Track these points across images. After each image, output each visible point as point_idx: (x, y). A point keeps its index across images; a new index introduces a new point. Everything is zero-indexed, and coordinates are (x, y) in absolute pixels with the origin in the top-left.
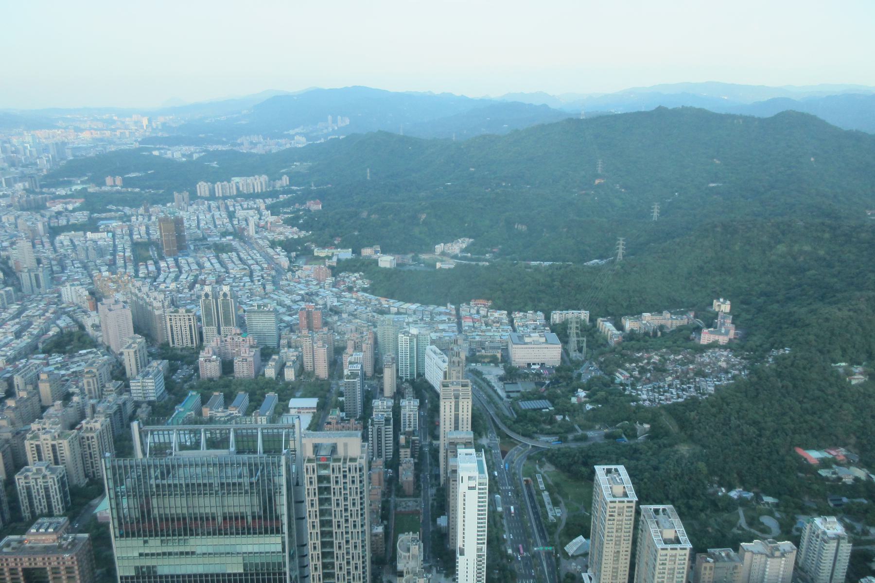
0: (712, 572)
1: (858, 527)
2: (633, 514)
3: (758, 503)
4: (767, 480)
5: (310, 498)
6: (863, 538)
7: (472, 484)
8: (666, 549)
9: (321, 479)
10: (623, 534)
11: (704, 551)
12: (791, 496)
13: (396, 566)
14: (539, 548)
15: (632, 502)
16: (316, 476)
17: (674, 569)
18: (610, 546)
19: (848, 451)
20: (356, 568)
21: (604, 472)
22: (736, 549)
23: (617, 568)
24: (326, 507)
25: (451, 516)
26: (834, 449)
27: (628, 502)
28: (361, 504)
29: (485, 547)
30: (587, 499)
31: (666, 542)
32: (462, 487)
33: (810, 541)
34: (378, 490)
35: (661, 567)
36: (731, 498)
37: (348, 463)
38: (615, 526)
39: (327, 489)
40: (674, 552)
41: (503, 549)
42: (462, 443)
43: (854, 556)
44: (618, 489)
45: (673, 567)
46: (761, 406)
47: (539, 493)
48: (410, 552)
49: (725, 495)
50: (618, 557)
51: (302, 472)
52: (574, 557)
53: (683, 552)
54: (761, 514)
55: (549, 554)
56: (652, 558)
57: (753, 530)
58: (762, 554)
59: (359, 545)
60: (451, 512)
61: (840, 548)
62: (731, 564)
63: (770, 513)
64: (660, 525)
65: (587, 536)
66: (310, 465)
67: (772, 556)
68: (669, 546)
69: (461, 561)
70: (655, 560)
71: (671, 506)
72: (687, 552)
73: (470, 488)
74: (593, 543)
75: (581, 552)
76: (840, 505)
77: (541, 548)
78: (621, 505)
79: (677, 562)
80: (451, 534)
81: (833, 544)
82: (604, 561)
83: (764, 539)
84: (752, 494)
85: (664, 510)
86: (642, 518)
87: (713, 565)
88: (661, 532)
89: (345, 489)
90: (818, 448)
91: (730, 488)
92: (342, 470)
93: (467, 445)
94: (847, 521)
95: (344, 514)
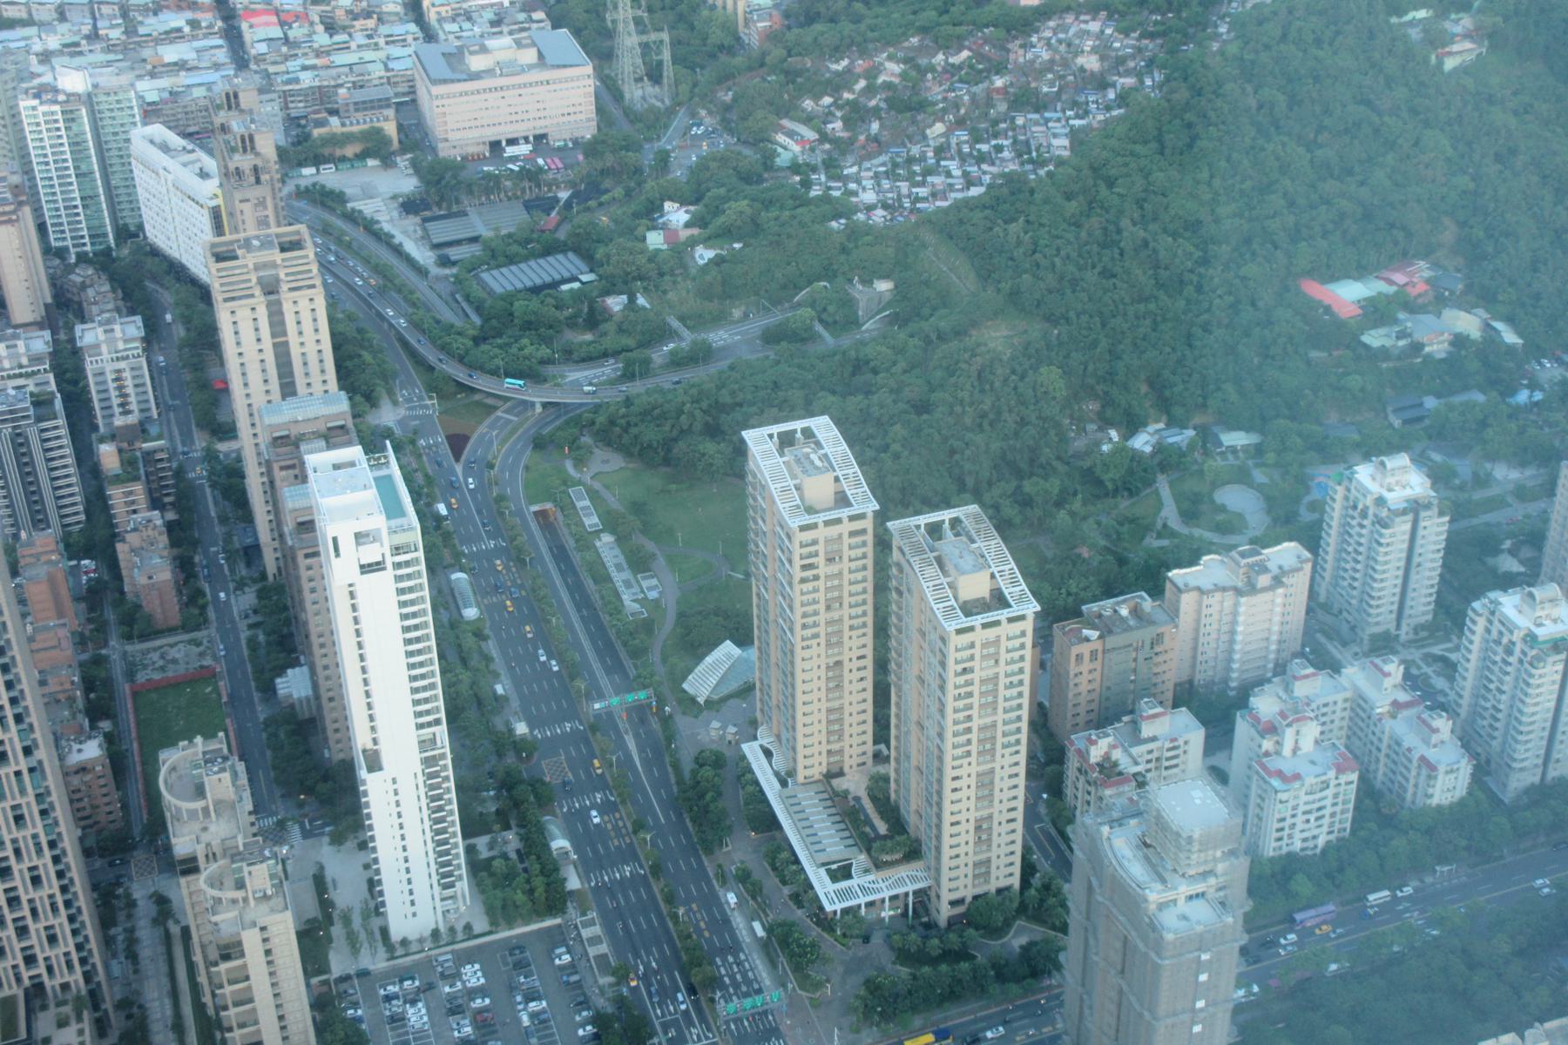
0: (1097, 665)
1: (1464, 468)
2: (869, 550)
3: (1206, 453)
4: (1229, 388)
6: (1477, 496)
7: (371, 554)
8: (971, 629)
10: (846, 611)
12: (1293, 418)
13: (168, 848)
14: (611, 702)
15: (862, 516)
17: (996, 676)
18: (814, 651)
19: (1436, 265)
20: (36, 881)
21: (772, 446)
22: (1156, 589)
23: (841, 708)
25: (320, 663)
26: (1397, 270)
27: (852, 518)
29: (442, 732)
31: (969, 609)
32: (341, 571)
33: (1345, 532)
35: (961, 680)
36: (1136, 456)
38: (821, 596)
40: (991, 633)
42: (318, 435)
43: (1454, 548)
44: (820, 488)
45: (991, 673)
46: (1205, 175)
47: (585, 541)
48: (206, 795)
49: (1120, 450)
53: (1017, 627)
54: (1215, 485)
55: (639, 711)
56: (935, 661)
57: (1197, 532)
58: (1224, 589)
59: (31, 808)
60: (317, 652)
61: (1421, 532)
62: (1147, 634)
63: (1241, 477)
64: (949, 567)
65: (743, 640)
67: (1251, 589)
68: (977, 621)
69: (374, 787)
70: (943, 664)
72: (1028, 626)
73: (367, 569)
74: (764, 654)
75: (734, 685)
76: (1420, 419)
77: (615, 701)
78: (833, 531)
80: (329, 717)
81: (1403, 527)
82: (800, 699)
84: (1190, 433)
85: (955, 522)
86: (896, 554)
87: (1098, 645)
88: (952, 586)
90: (1360, 271)
91: (1132, 425)
93: (332, 436)
94: (1437, 457)
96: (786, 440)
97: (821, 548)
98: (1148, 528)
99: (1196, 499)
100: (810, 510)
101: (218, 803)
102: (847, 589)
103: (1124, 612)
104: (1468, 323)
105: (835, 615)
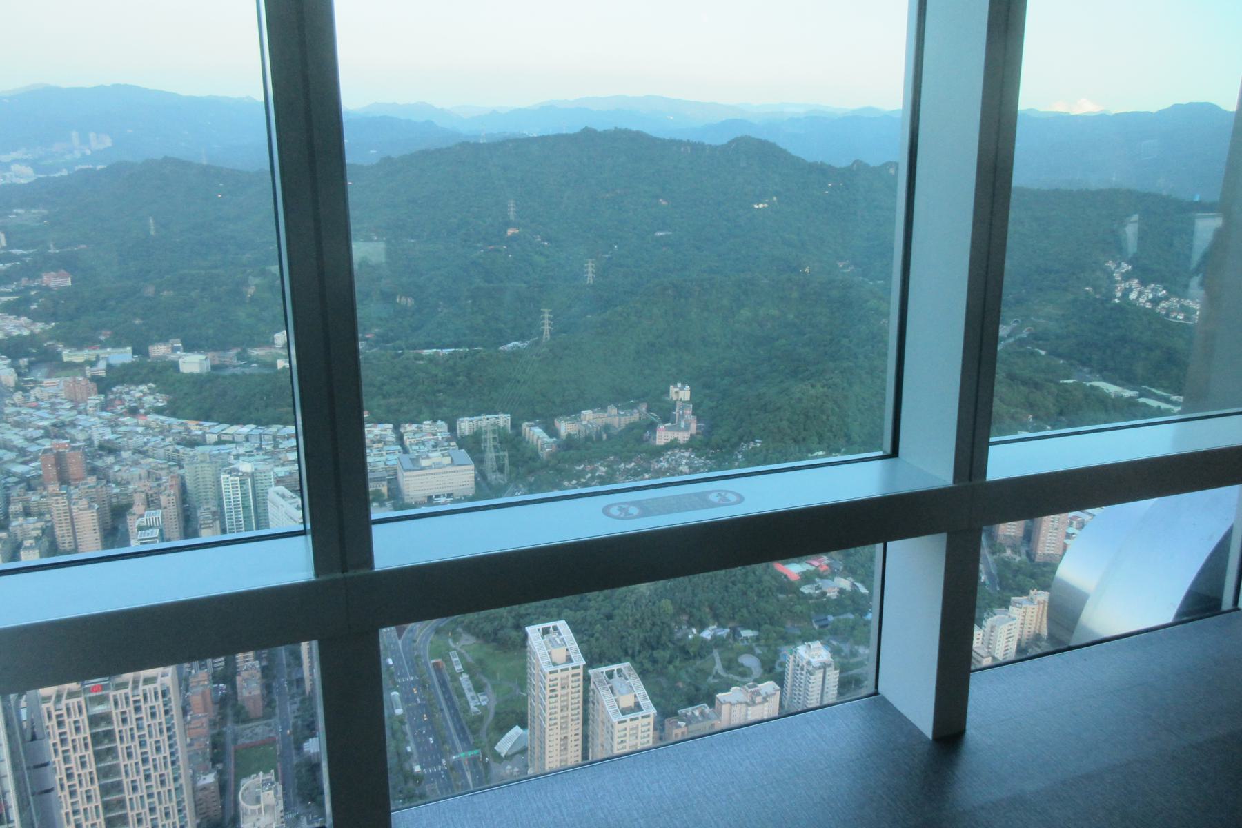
1: (846, 648)
2: (581, 683)
3: (735, 640)
4: (744, 610)
5: (79, 754)
6: (853, 660)
9: (94, 720)
10: (570, 712)
11: (675, 714)
12: (772, 624)
14: (462, 756)
16: (85, 716)
21: (539, 634)
22: (711, 701)
24: (109, 762)
28: (171, 746)
30: (521, 677)
31: (624, 712)
34: (202, 718)
36: (704, 641)
37: (141, 687)
38: (558, 705)
39: (109, 735)
40: (634, 723)
41: (407, 767)
44: (560, 654)
47: (455, 678)
49: (696, 638)
50: (566, 744)
51: (40, 717)
52: (509, 757)
53: (646, 721)
54: (740, 653)
55: (474, 761)
57: (731, 676)
63: (750, 651)
65: (524, 725)
66: (73, 702)
67: (753, 703)
68: (628, 717)
71: (628, 664)
72: (651, 720)
74: (532, 732)
75: (519, 748)
76: (826, 625)
77: (462, 755)
78: (565, 674)
79: (640, 735)
81: (819, 674)
83: (745, 683)
84: (728, 630)
85: (619, 671)
89: (139, 728)
91: (702, 626)
92: (131, 699)
94: (834, 643)
95: (142, 768)
96: (546, 631)
97: (559, 682)
98: (709, 674)
99: (730, 661)
100: (554, 664)
101: (267, 808)
102: (570, 701)
103: (697, 713)
104: (845, 583)
105: (565, 714)
